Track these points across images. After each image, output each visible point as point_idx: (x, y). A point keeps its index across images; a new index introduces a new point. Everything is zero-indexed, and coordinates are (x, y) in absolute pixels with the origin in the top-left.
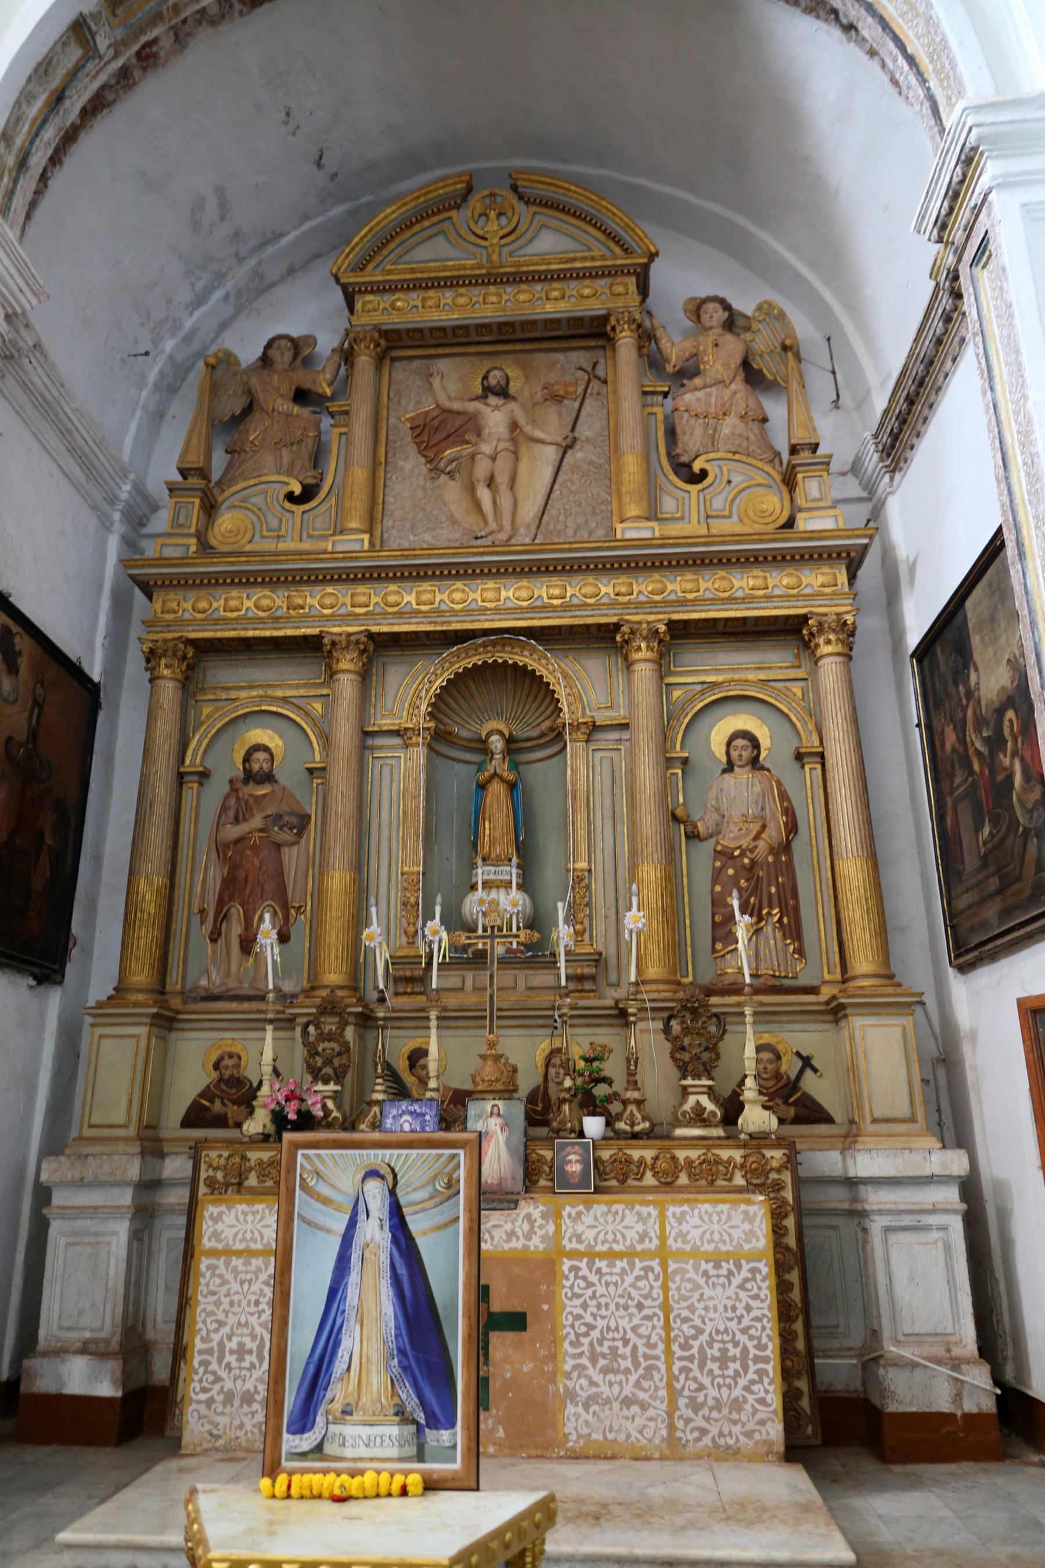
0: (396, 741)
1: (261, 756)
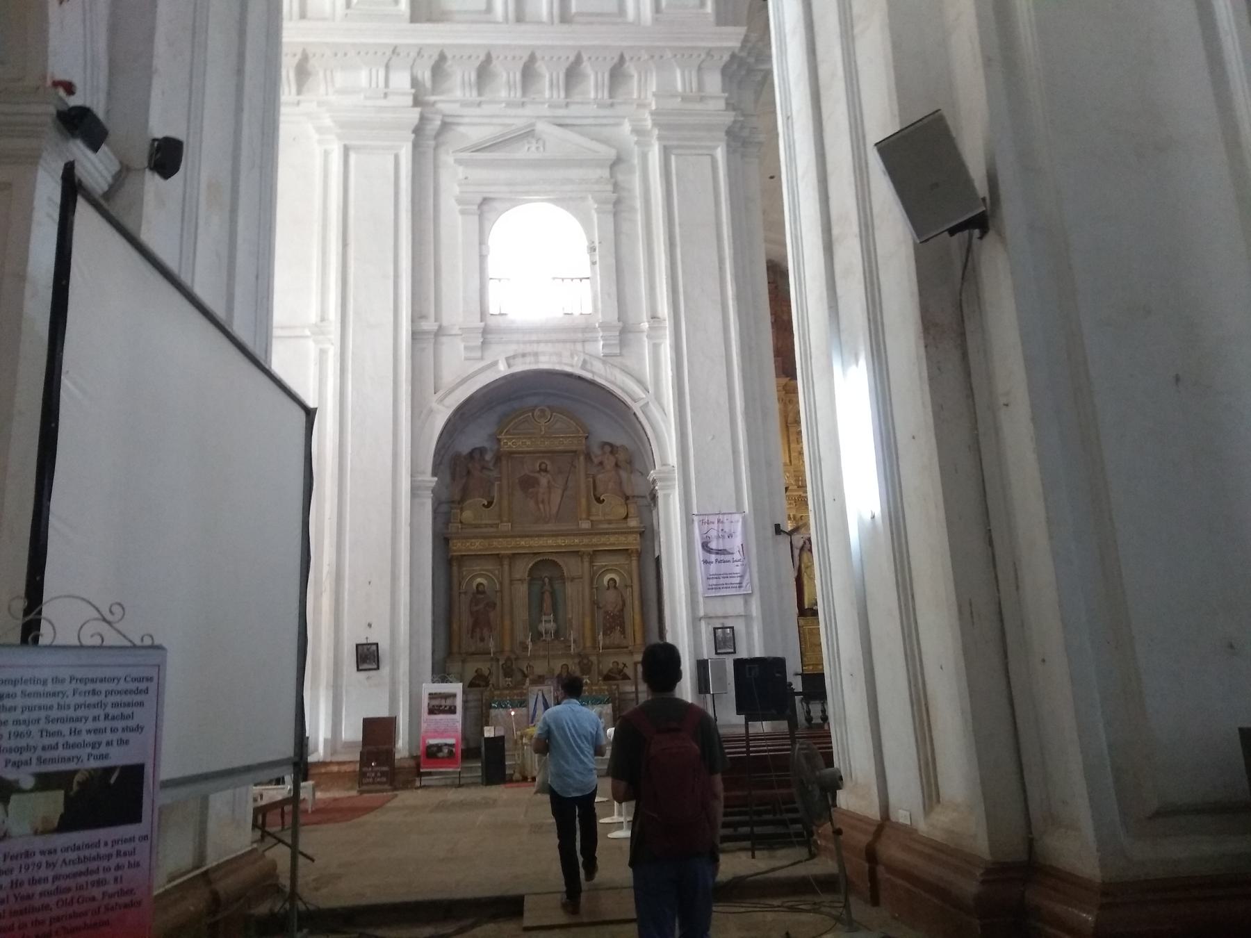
0: (520, 582)
1: (482, 586)
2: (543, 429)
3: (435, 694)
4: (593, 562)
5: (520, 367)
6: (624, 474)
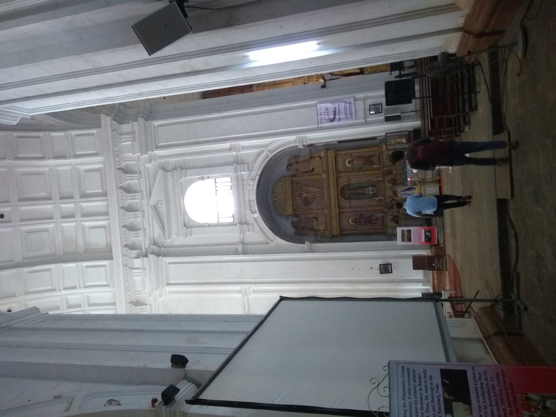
0: (351, 204)
1: (353, 221)
2: (282, 196)
3: (402, 239)
4: (341, 171)
5: (256, 208)
6: (301, 159)
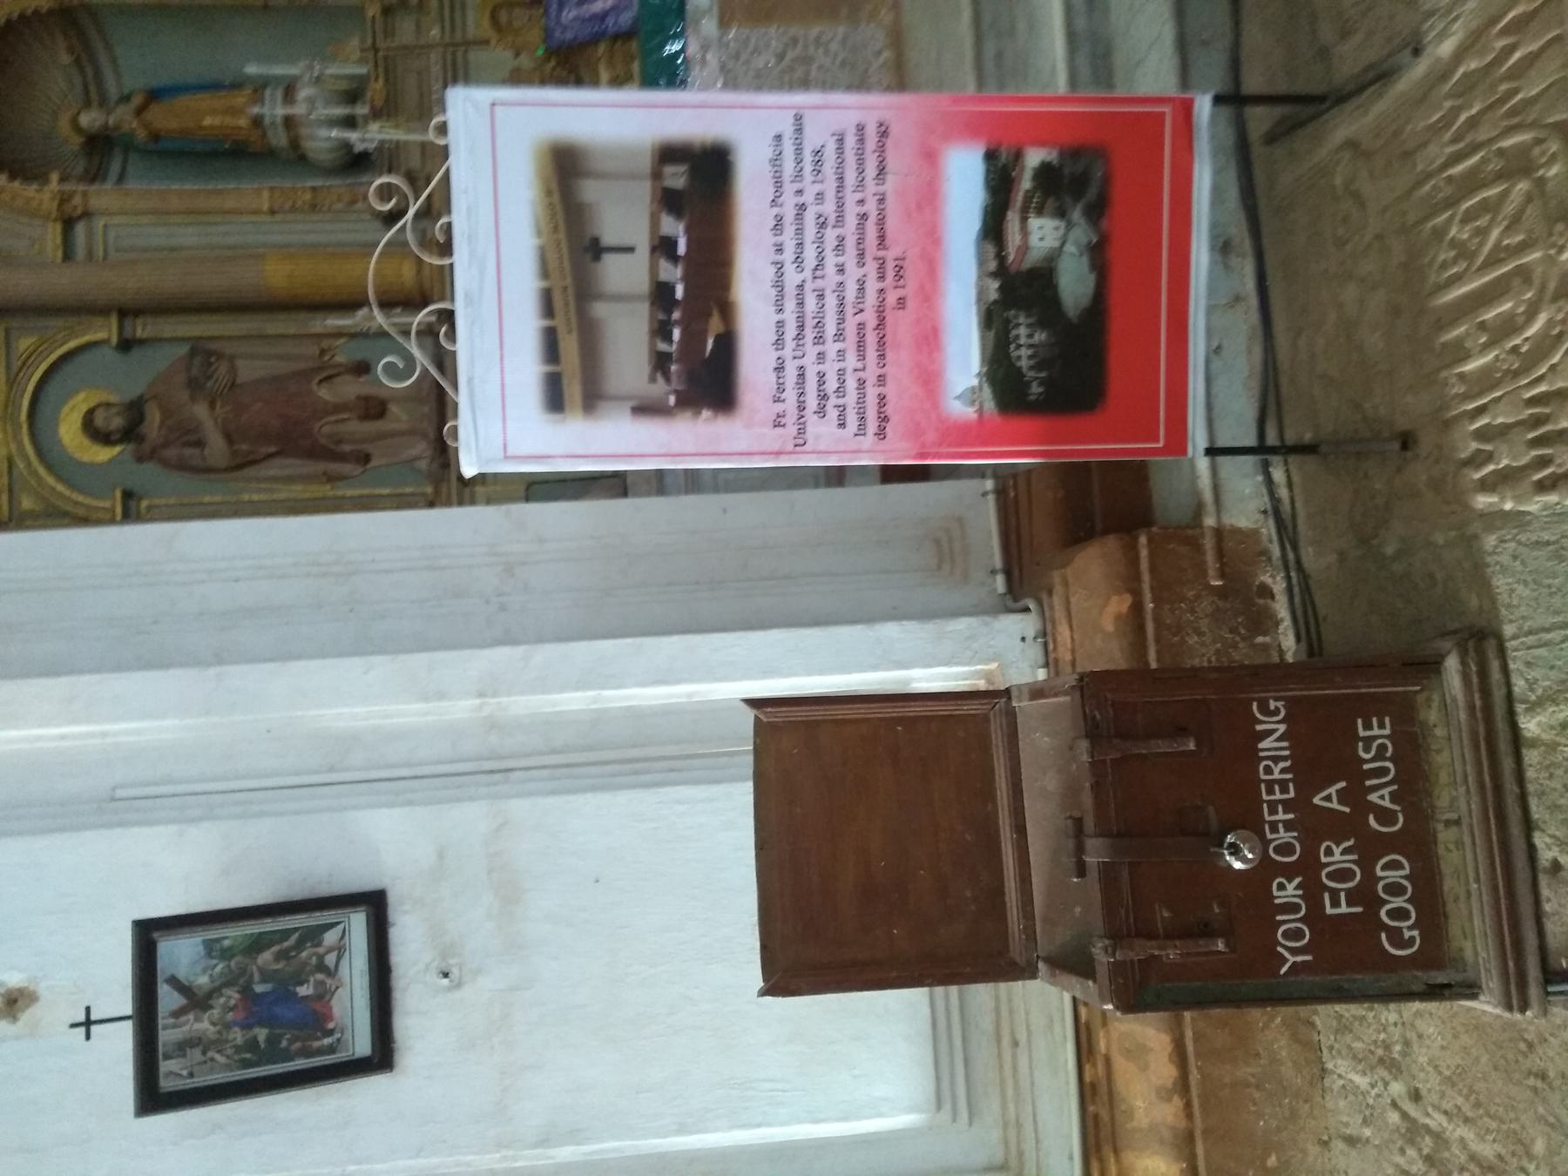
3: (551, 347)
